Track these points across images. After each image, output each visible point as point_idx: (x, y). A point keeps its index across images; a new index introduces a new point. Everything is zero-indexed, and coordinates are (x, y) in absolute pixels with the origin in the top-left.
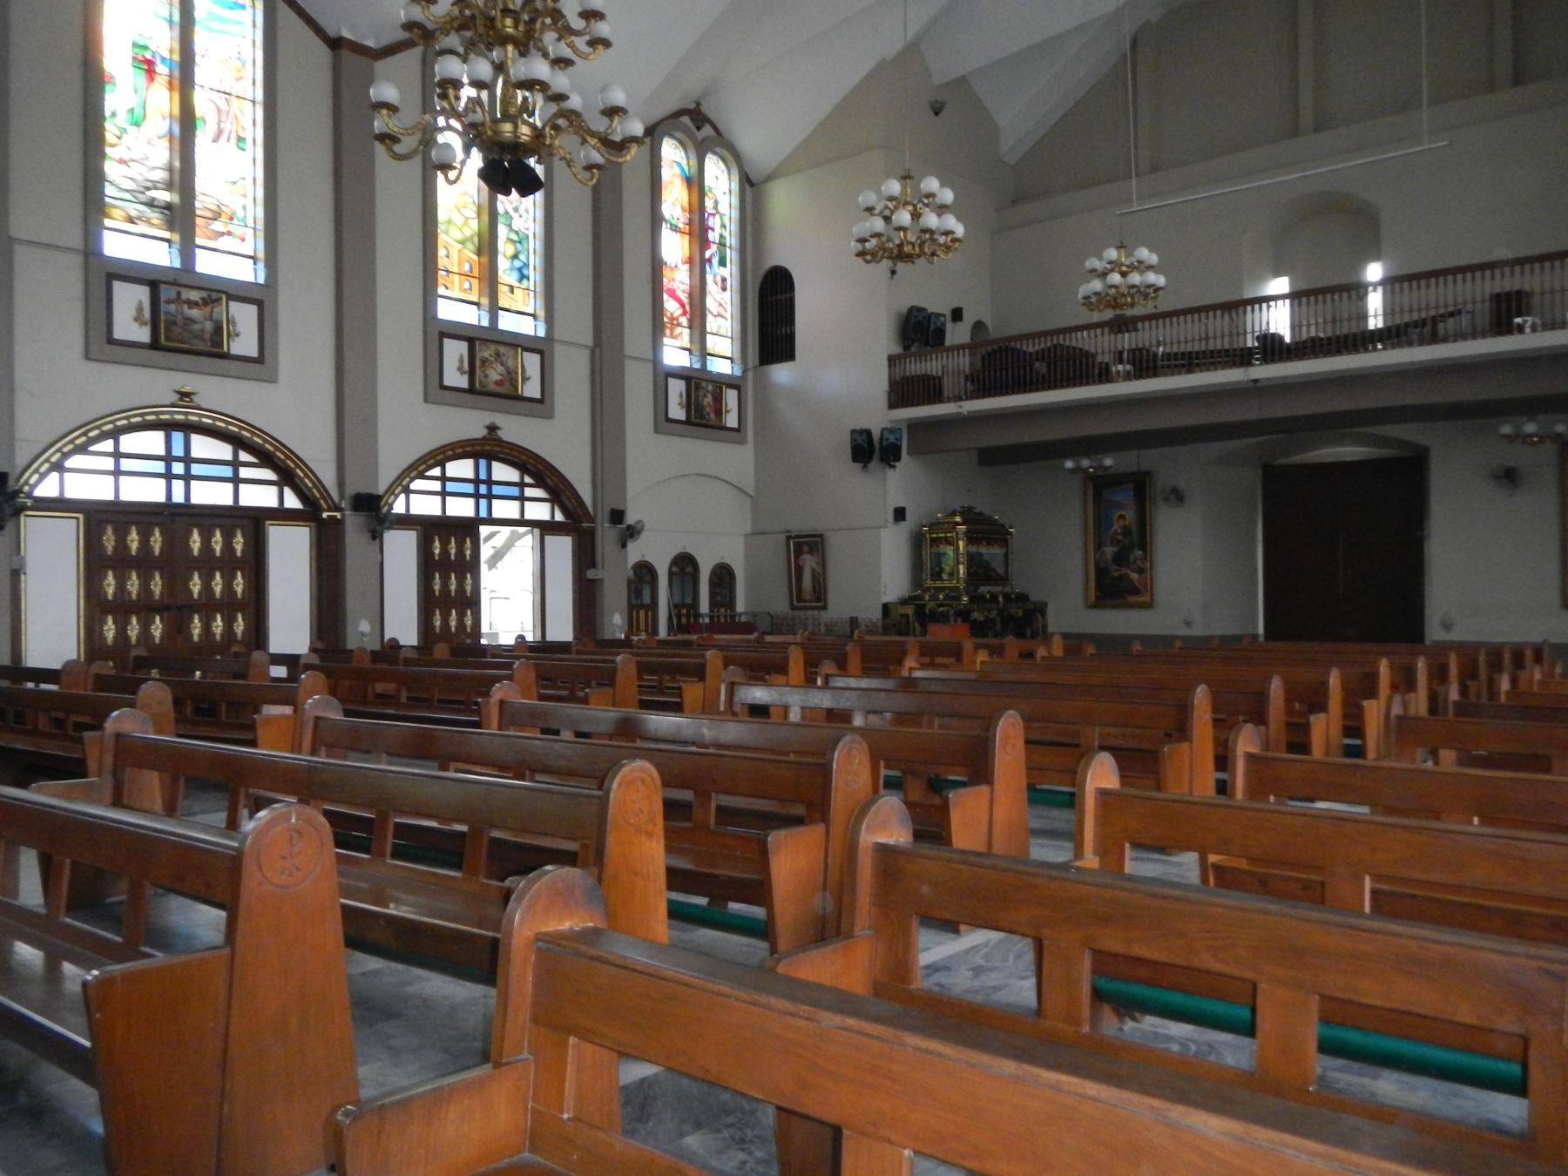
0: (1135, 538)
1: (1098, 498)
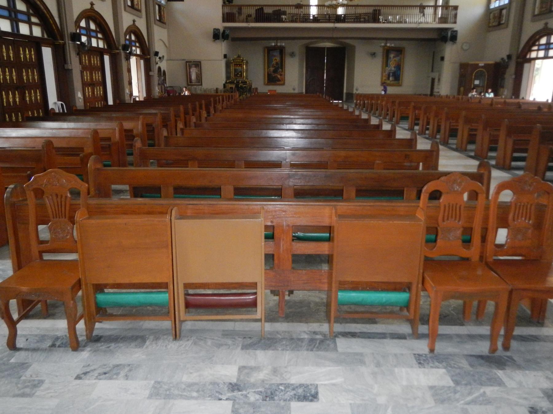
0: (279, 66)
1: (268, 53)
